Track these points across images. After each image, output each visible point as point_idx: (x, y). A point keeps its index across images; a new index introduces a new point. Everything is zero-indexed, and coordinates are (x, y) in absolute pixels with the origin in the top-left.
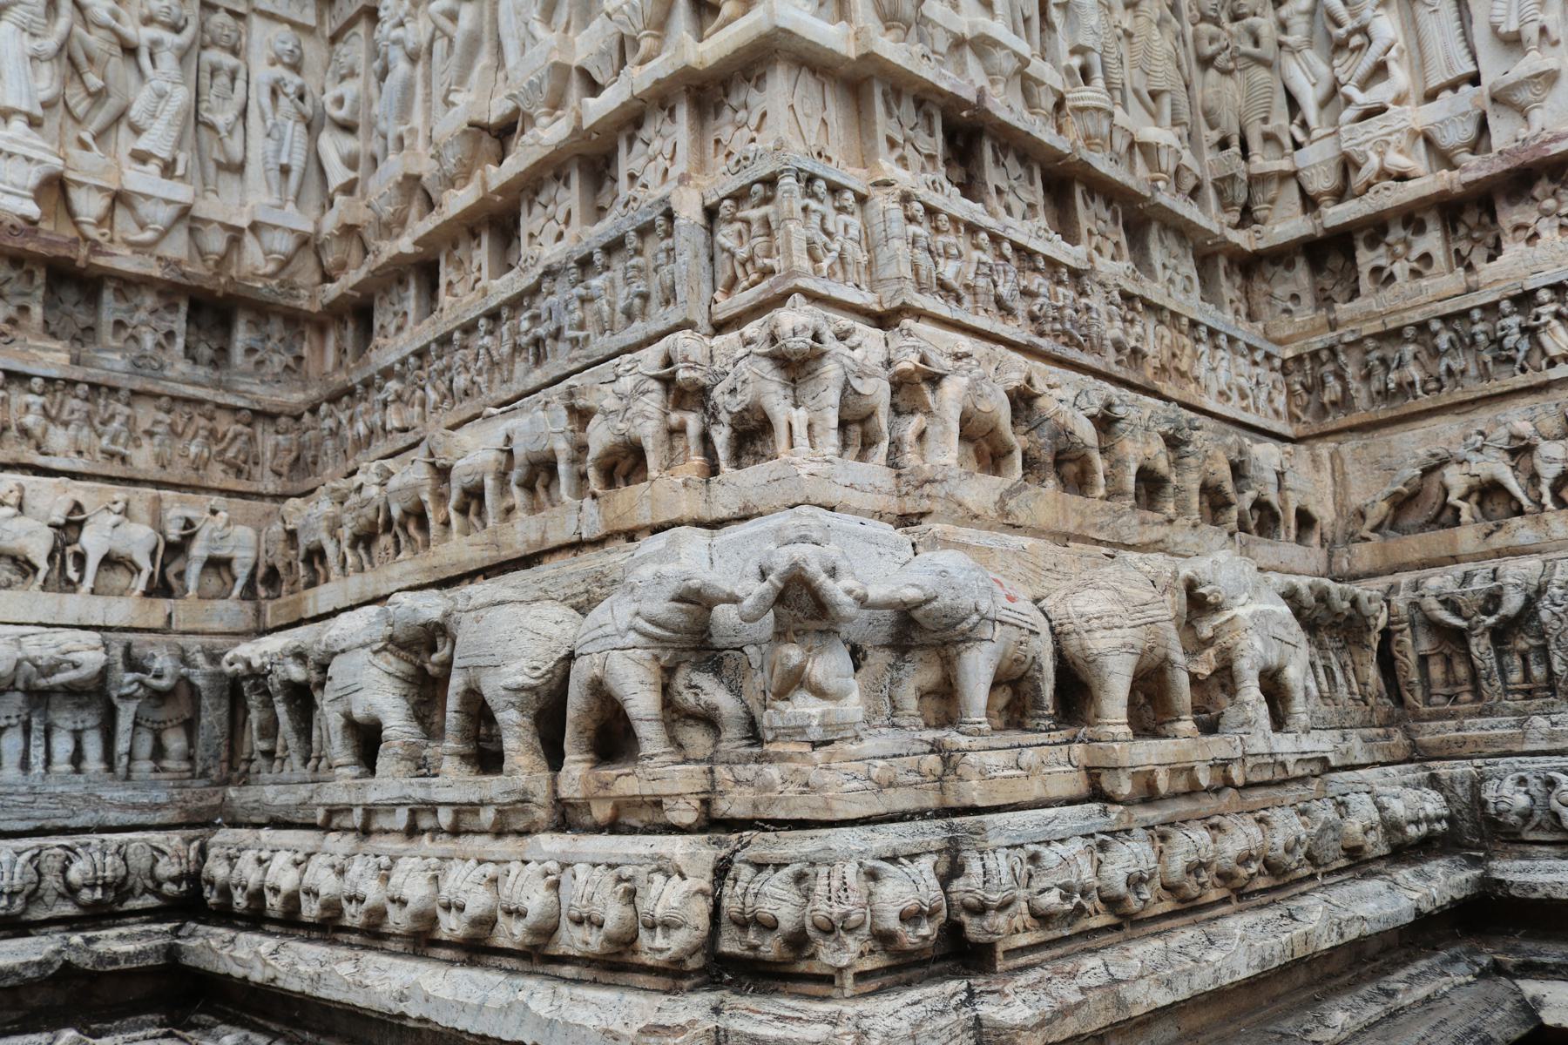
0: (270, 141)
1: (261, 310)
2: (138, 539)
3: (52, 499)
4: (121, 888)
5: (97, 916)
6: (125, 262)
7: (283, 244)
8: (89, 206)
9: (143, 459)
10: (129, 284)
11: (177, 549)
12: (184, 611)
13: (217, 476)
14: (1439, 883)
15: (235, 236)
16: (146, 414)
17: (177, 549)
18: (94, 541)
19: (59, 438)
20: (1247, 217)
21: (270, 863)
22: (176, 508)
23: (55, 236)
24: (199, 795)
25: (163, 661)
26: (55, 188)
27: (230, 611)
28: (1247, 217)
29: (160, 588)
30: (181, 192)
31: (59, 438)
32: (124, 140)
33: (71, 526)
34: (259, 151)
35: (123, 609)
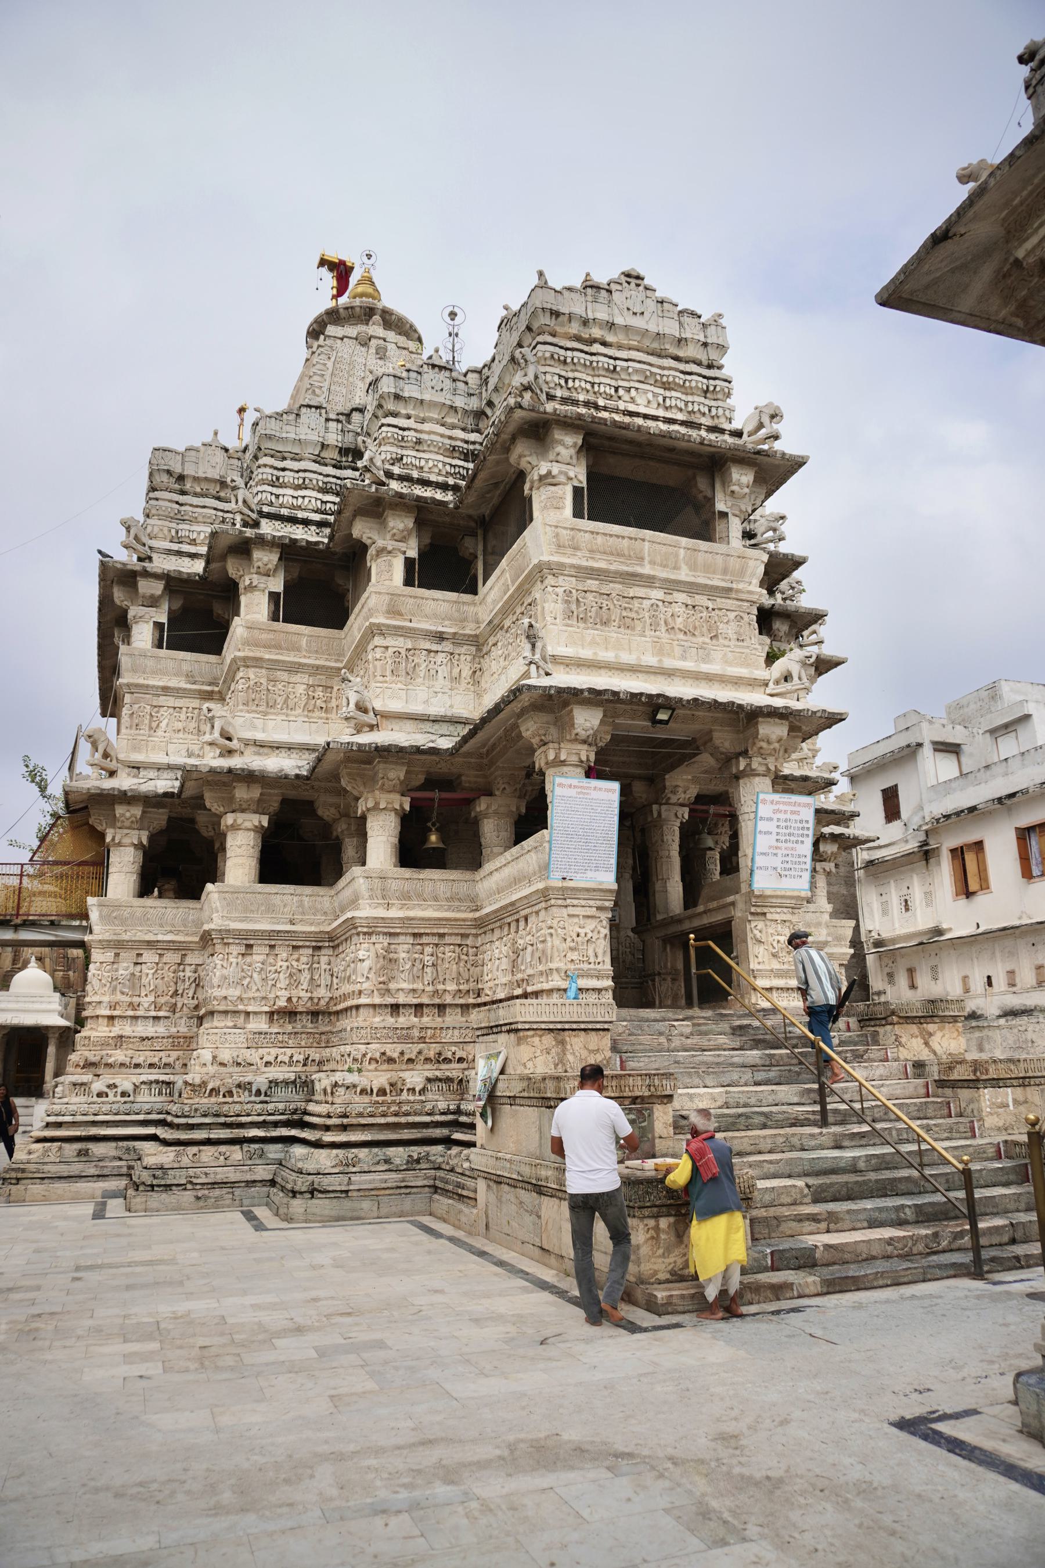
0: (324, 979)
1: (323, 1013)
2: (301, 1058)
3: (289, 1052)
4: (296, 1110)
5: (293, 1113)
6: (300, 1009)
7: (327, 1000)
8: (294, 1000)
9: (303, 1043)
10: (301, 1013)
11: (307, 1059)
12: (308, 1068)
13: (315, 1045)
14: (450, 1117)
15: (319, 999)
16: (304, 1036)
17: (307, 1059)
18: (295, 1059)
19: (290, 1042)
20: (479, 996)
21: (312, 1107)
22: (308, 1051)
23: (289, 1008)
24: (308, 1097)
25: (303, 1078)
26: (289, 999)
27: (315, 1068)
28: (479, 996)
29: (305, 1065)
30: (309, 995)
31: (290, 1042)
32: (300, 987)
33: (291, 1057)
34: (323, 982)
35: (298, 1069)
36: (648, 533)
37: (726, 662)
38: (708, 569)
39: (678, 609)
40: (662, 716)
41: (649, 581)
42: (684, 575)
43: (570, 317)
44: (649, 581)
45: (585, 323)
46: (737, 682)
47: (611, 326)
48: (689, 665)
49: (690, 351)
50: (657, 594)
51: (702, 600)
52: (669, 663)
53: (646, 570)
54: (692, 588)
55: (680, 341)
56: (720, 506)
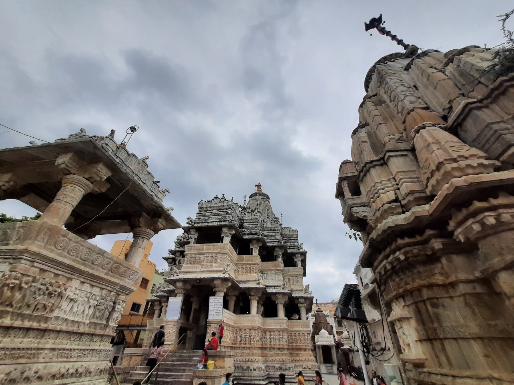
36: (205, 244)
37: (216, 267)
38: (217, 249)
39: (209, 258)
40: (198, 281)
41: (204, 253)
42: (212, 251)
43: (204, 208)
44: (204, 253)
45: (206, 208)
46: (216, 272)
47: (210, 207)
48: (206, 269)
49: (225, 207)
50: (206, 255)
51: (214, 255)
52: (202, 270)
53: (204, 251)
54: (212, 253)
55: (223, 206)
56: (222, 235)
